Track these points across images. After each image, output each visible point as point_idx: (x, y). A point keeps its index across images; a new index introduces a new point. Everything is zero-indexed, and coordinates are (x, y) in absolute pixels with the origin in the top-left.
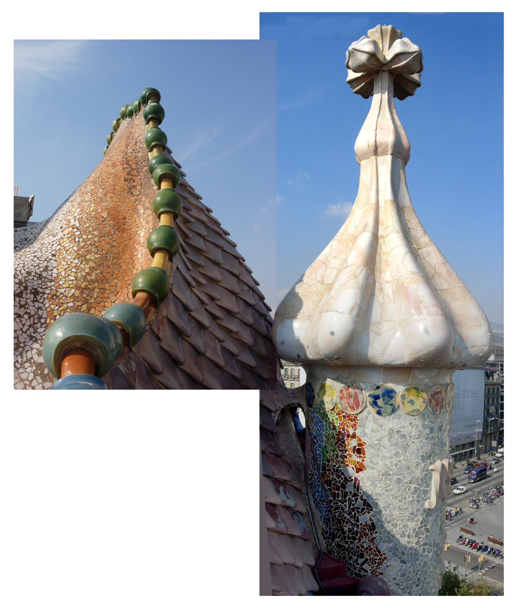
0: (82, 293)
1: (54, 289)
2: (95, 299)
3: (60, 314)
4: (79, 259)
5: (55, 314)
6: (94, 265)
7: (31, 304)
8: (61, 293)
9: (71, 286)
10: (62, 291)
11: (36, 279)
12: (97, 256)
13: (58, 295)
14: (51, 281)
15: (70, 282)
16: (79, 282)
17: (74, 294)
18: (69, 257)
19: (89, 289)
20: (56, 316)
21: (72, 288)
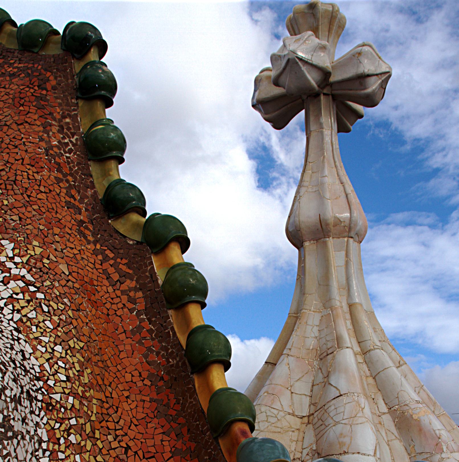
0: (81, 403)
1: (46, 393)
2: (96, 414)
3: (63, 436)
4: (60, 345)
5: (58, 436)
6: (82, 360)
7: (29, 416)
8: (57, 401)
9: (67, 391)
10: (57, 397)
11: (23, 373)
12: (82, 344)
13: (54, 404)
14: (38, 379)
15: (63, 385)
16: (74, 385)
17: (73, 405)
18: (46, 339)
19: (87, 398)
20: (59, 439)
21: (69, 394)
